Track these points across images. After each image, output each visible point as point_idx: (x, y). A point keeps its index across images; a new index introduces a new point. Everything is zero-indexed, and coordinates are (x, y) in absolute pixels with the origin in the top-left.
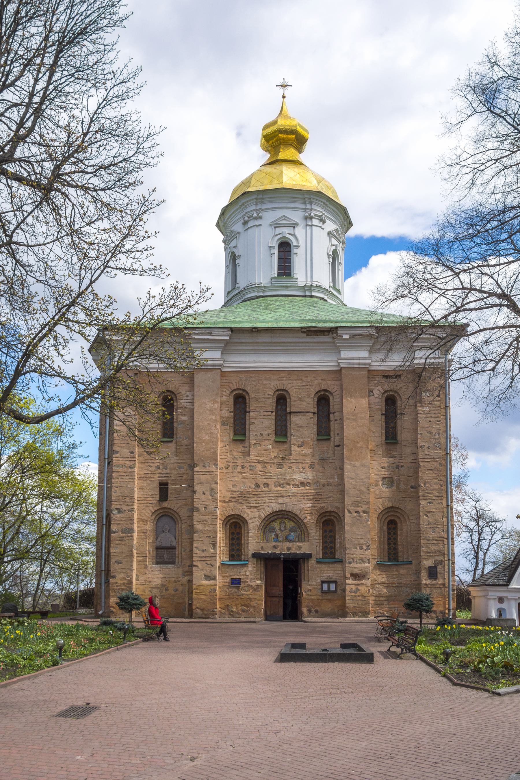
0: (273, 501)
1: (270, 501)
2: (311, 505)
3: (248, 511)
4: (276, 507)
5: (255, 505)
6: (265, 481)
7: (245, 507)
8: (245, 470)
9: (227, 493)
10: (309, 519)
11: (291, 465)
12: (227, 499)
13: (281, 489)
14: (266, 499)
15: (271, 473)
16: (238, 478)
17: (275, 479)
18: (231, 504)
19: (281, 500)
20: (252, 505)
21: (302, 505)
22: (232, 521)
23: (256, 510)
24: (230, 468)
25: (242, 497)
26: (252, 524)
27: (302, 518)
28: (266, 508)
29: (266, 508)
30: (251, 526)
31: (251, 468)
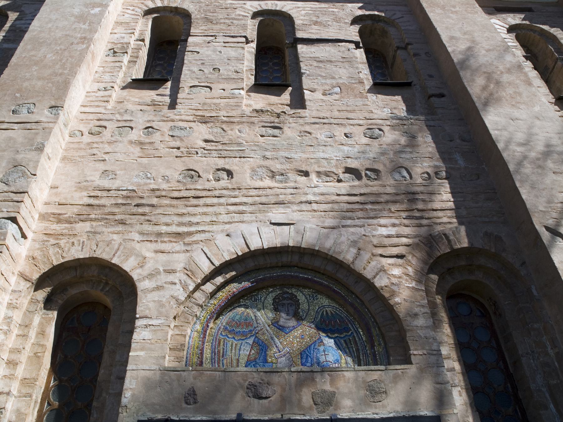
0: (247, 217)
1: (237, 217)
2: (393, 231)
3: (147, 250)
4: (262, 236)
5: (174, 229)
6: (221, 163)
7: (137, 237)
8: (156, 137)
9: (77, 195)
10: (398, 279)
11: (307, 128)
12: (70, 212)
13: (276, 185)
14: (222, 209)
15: (239, 144)
16: (125, 151)
17: (255, 160)
18: (83, 227)
19: (277, 214)
20: (164, 229)
21: (358, 230)
22: (73, 291)
23: (178, 247)
24: (107, 134)
25: (133, 206)
26: (155, 296)
27: (368, 274)
28: (221, 240)
29: (221, 240)
30: (146, 303)
31: (177, 133)
